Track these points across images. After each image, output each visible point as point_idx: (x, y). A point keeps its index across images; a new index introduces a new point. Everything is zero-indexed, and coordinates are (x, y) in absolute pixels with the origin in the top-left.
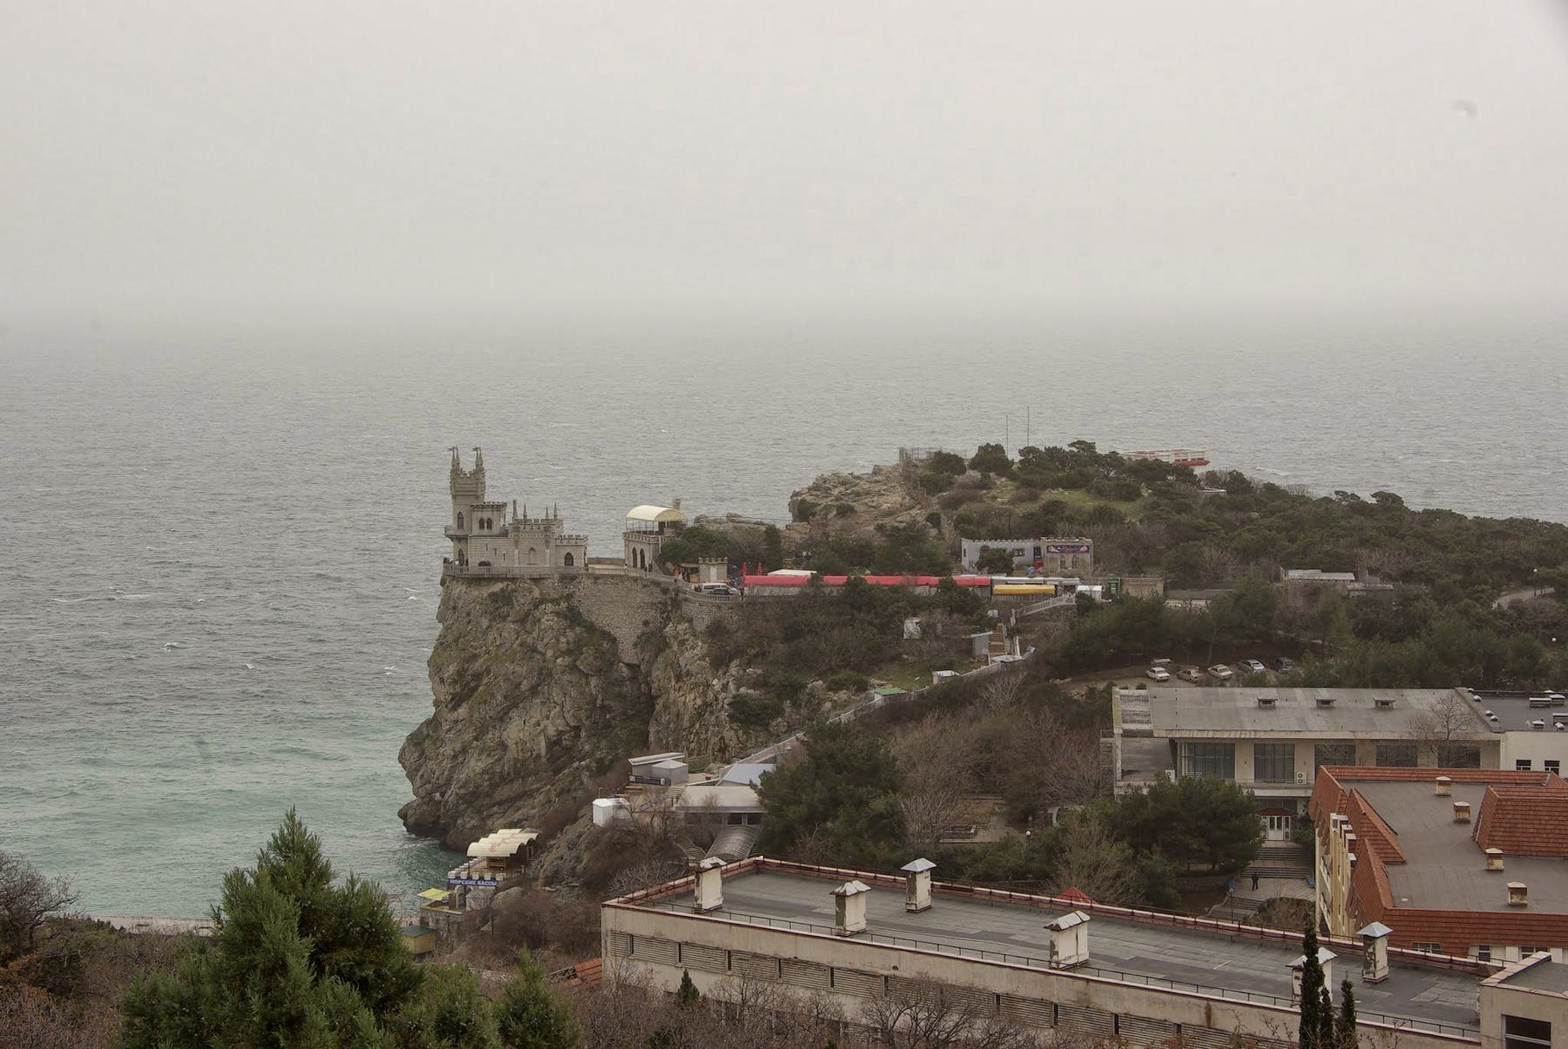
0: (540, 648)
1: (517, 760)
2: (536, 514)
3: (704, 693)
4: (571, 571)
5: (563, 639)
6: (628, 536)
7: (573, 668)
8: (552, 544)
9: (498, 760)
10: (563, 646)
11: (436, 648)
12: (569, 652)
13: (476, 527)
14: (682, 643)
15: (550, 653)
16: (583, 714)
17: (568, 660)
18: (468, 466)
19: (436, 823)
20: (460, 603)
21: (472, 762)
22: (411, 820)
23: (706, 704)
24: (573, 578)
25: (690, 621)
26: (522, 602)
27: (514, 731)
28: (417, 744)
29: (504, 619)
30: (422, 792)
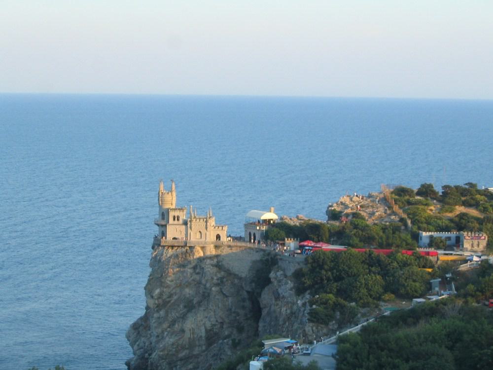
0: (203, 282)
3: (291, 308)
4: (219, 243)
9: (180, 339)
10: (215, 281)
12: (218, 285)
14: (279, 281)
15: (208, 285)
21: (167, 339)
23: (292, 313)
25: (284, 270)
27: (189, 324)
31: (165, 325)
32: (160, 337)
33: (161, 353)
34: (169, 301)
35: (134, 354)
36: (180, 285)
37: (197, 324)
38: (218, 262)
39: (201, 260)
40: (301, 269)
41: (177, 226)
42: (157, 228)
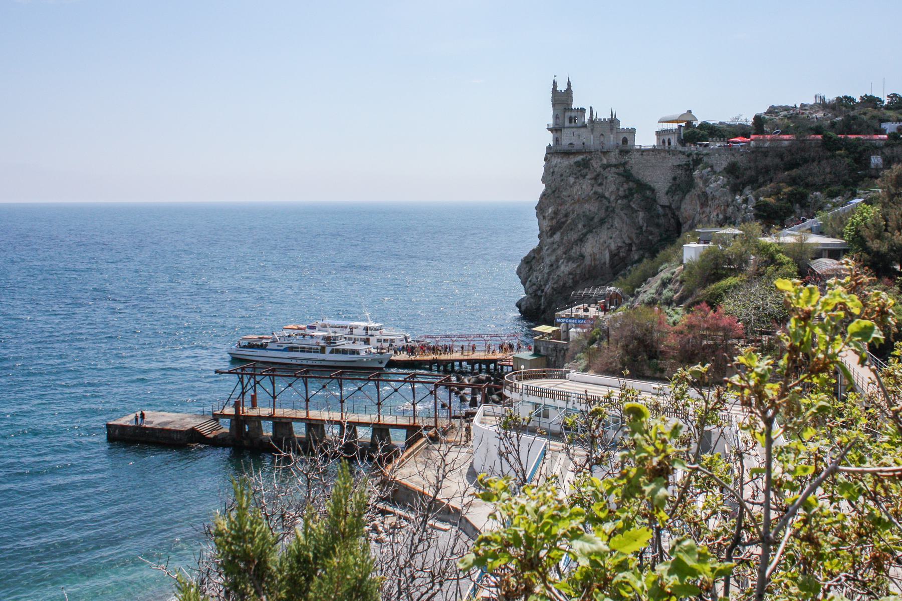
0: (607, 195)
1: (590, 266)
2: (603, 114)
5: (621, 189)
8: (615, 131)
10: (621, 193)
11: (541, 198)
12: (625, 197)
15: (612, 198)
16: (634, 236)
18: (562, 87)
19: (538, 308)
21: (563, 268)
22: (523, 308)
24: (627, 152)
25: (712, 167)
26: (596, 164)
27: (590, 248)
28: (527, 263)
29: (584, 176)
30: (530, 291)
31: (560, 252)
32: (554, 266)
33: (555, 286)
36: (579, 200)
38: (625, 171)
41: (575, 129)
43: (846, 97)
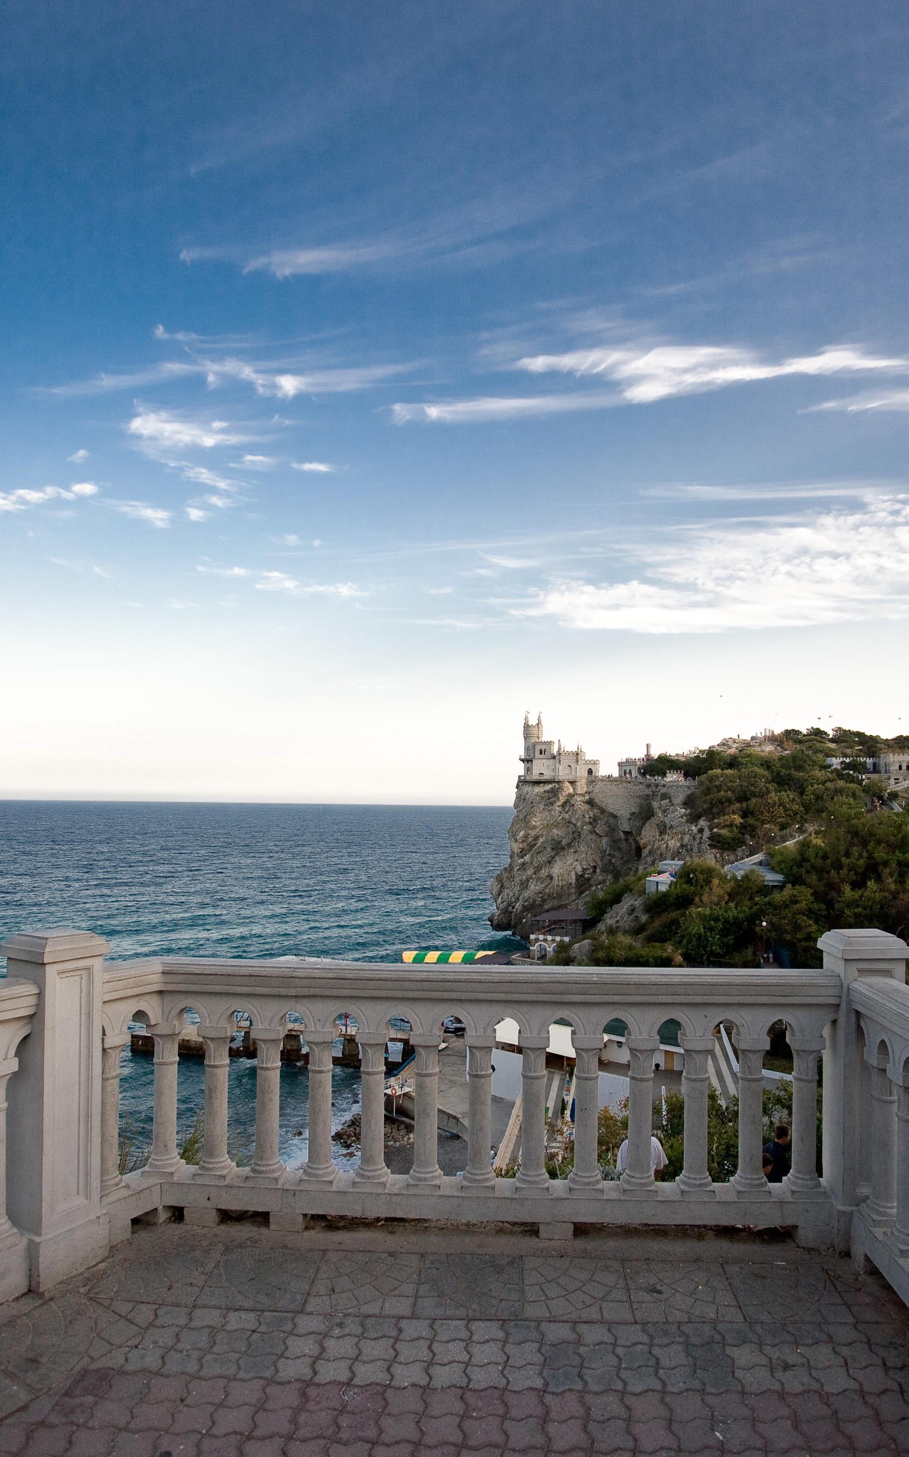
0: (574, 821)
1: (558, 885)
2: (570, 747)
3: (682, 839)
6: (620, 765)
7: (593, 832)
9: (547, 885)
10: (587, 820)
12: (590, 823)
13: (537, 753)
14: (665, 811)
15: (579, 824)
17: (589, 827)
20: (527, 797)
21: (532, 887)
22: (495, 922)
23: (682, 846)
25: (670, 798)
29: (552, 804)
31: (530, 872)
34: (535, 845)
35: (498, 908)
37: (565, 869)
39: (571, 796)
40: (693, 794)
42: (522, 765)
43: (793, 730)
